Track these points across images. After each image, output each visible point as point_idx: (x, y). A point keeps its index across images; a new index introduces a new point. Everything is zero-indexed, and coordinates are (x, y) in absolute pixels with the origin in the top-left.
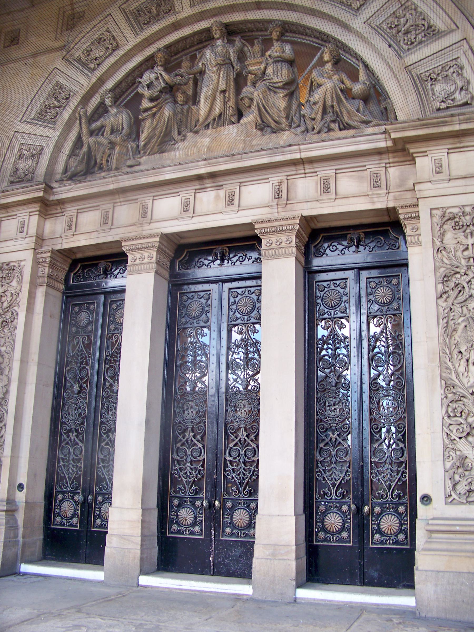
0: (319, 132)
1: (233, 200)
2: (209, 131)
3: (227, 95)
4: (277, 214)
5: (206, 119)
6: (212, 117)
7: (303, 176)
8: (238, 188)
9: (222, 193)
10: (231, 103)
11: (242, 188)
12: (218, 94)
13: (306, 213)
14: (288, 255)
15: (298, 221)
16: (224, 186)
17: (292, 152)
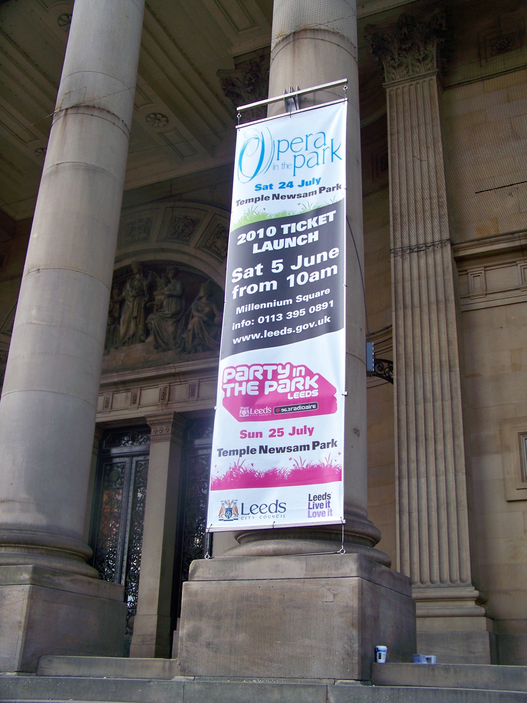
0: (189, 353)
1: (136, 400)
2: (125, 348)
3: (138, 320)
4: (161, 411)
5: (124, 338)
6: (127, 337)
7: (179, 383)
8: (139, 391)
9: (129, 394)
10: (141, 326)
11: (143, 391)
12: (132, 320)
13: (178, 410)
14: (165, 440)
15: (172, 416)
16: (131, 390)
17: (170, 368)
